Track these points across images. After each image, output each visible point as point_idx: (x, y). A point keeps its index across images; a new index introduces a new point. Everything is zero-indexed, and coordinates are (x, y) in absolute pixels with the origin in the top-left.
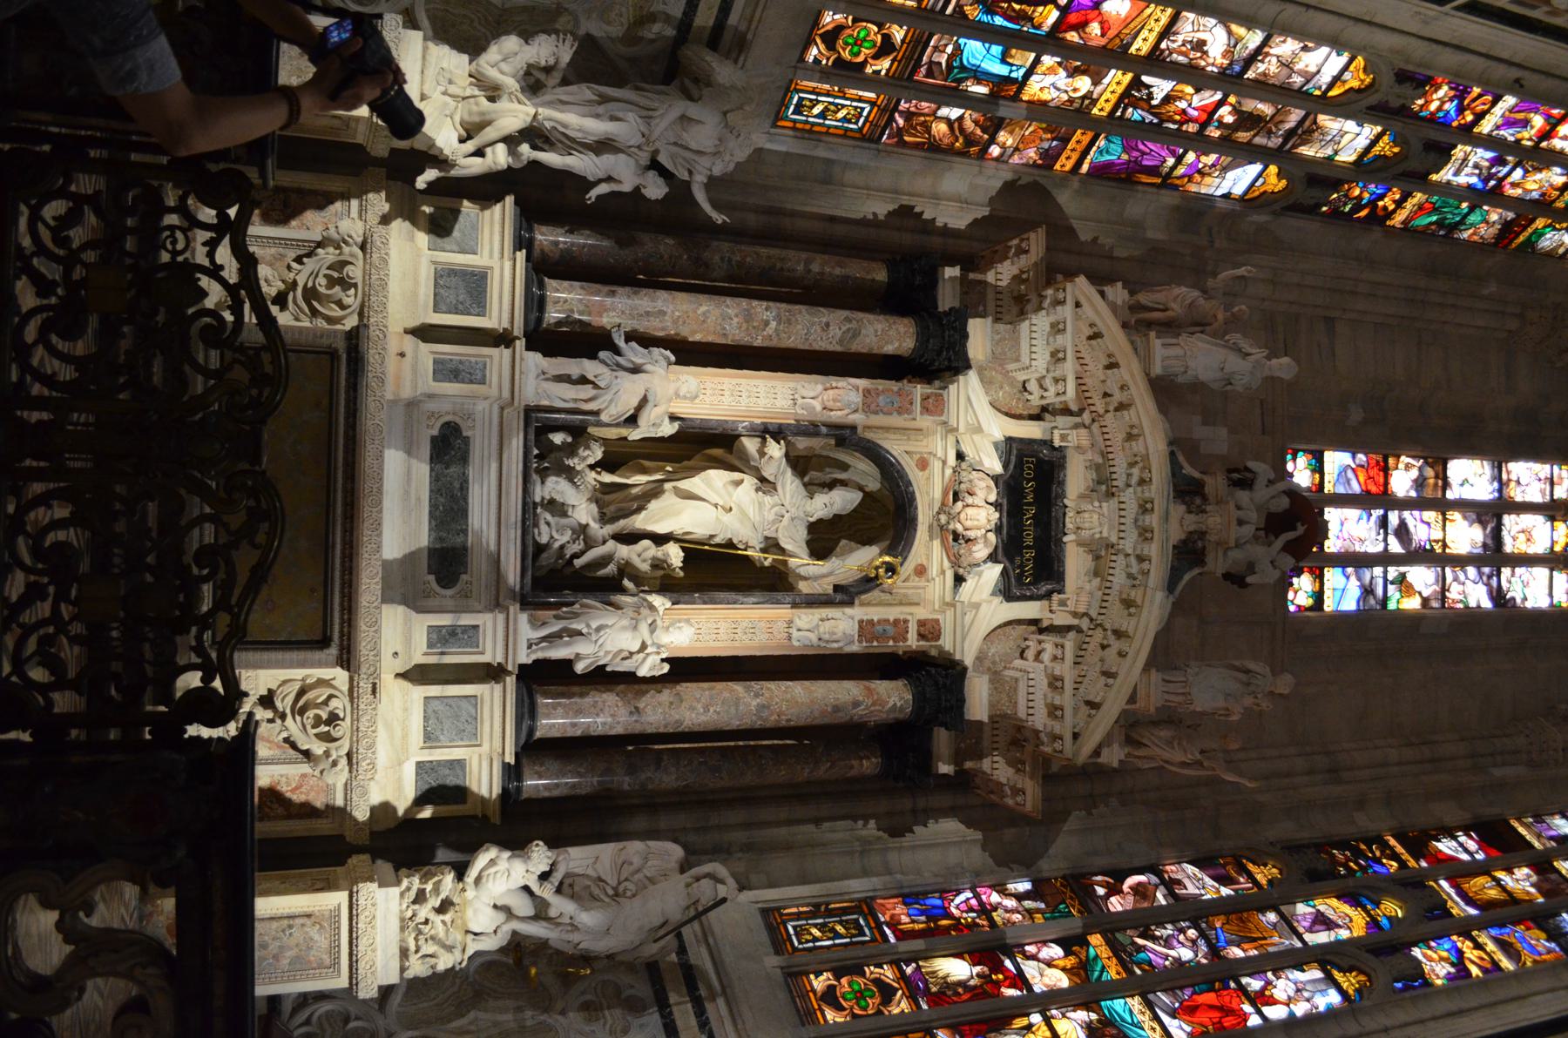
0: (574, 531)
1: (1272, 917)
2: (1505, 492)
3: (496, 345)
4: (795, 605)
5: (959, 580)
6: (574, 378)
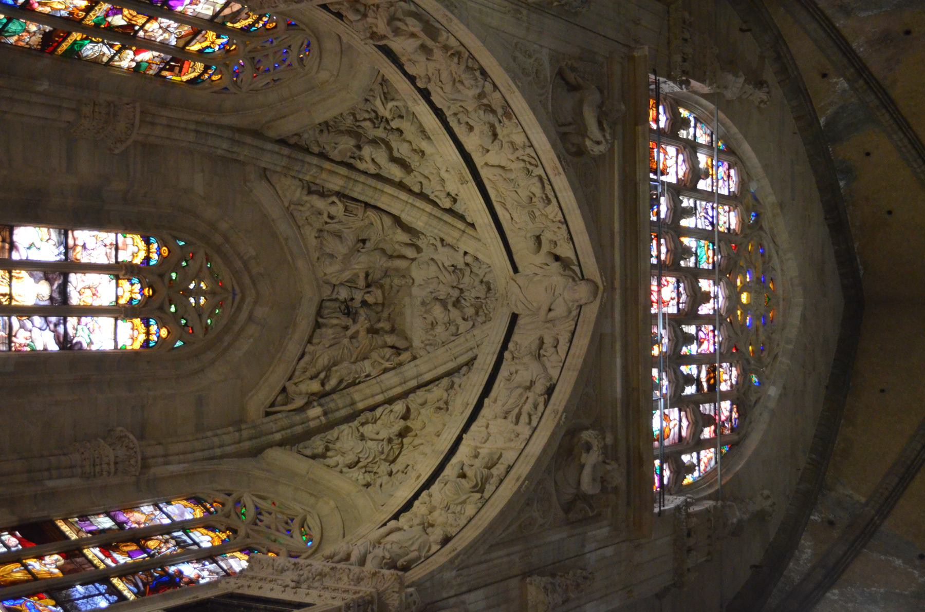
2: (71, 254)
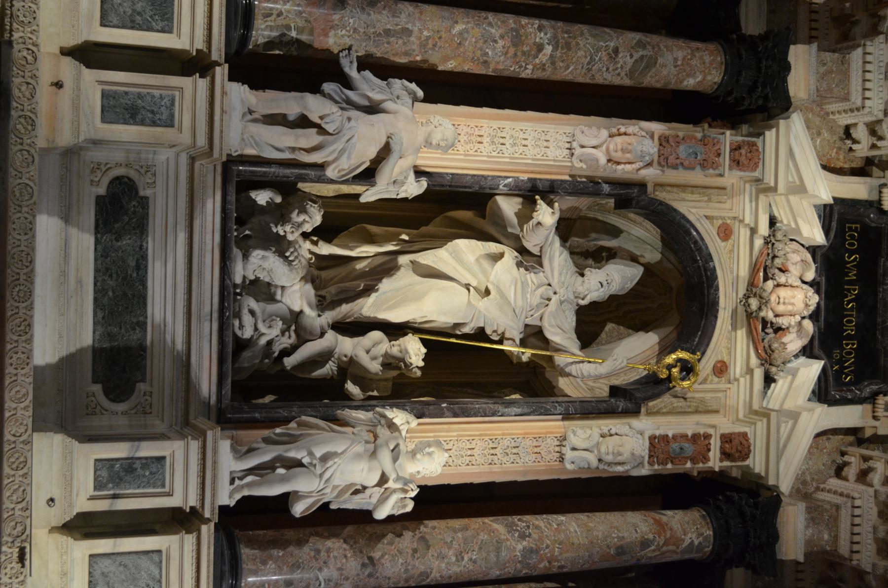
0: (283, 319)
4: (567, 416)
5: (769, 380)
6: (291, 118)
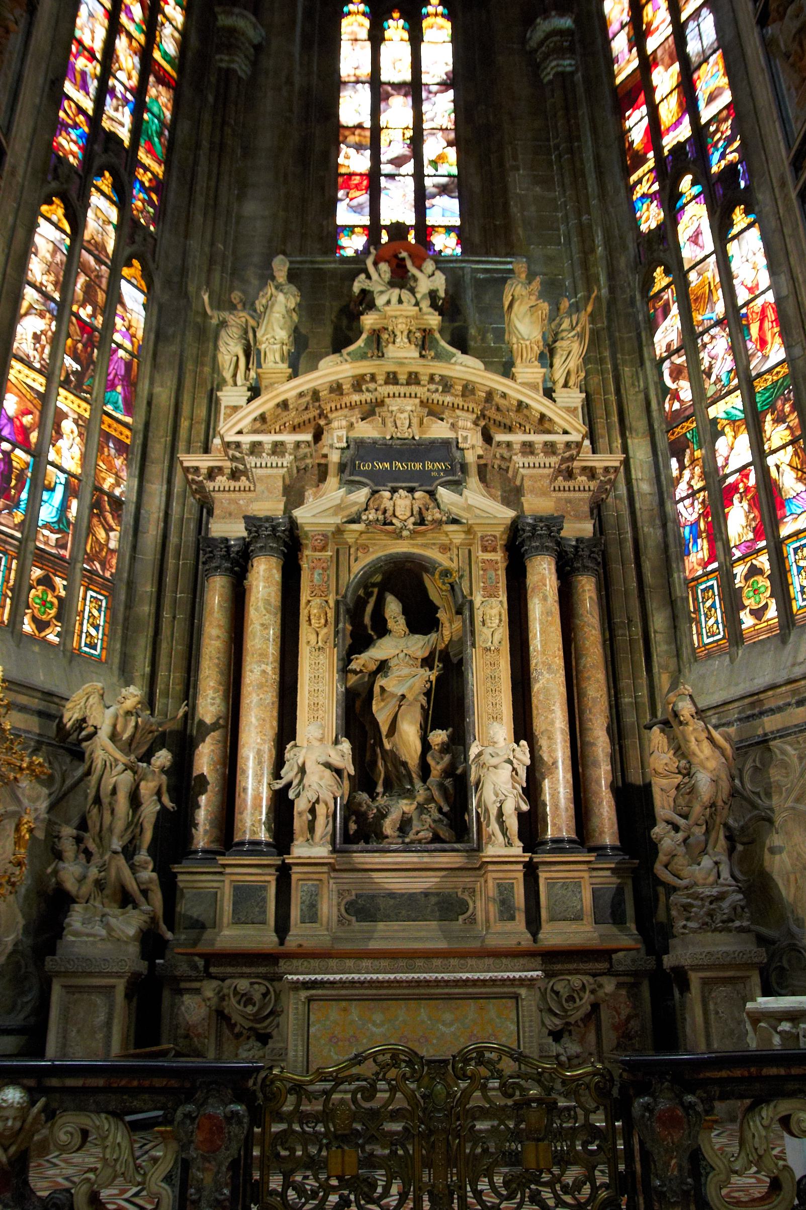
0: (421, 813)
1: (693, 276)
2: (363, 79)
3: (289, 877)
4: (473, 645)
